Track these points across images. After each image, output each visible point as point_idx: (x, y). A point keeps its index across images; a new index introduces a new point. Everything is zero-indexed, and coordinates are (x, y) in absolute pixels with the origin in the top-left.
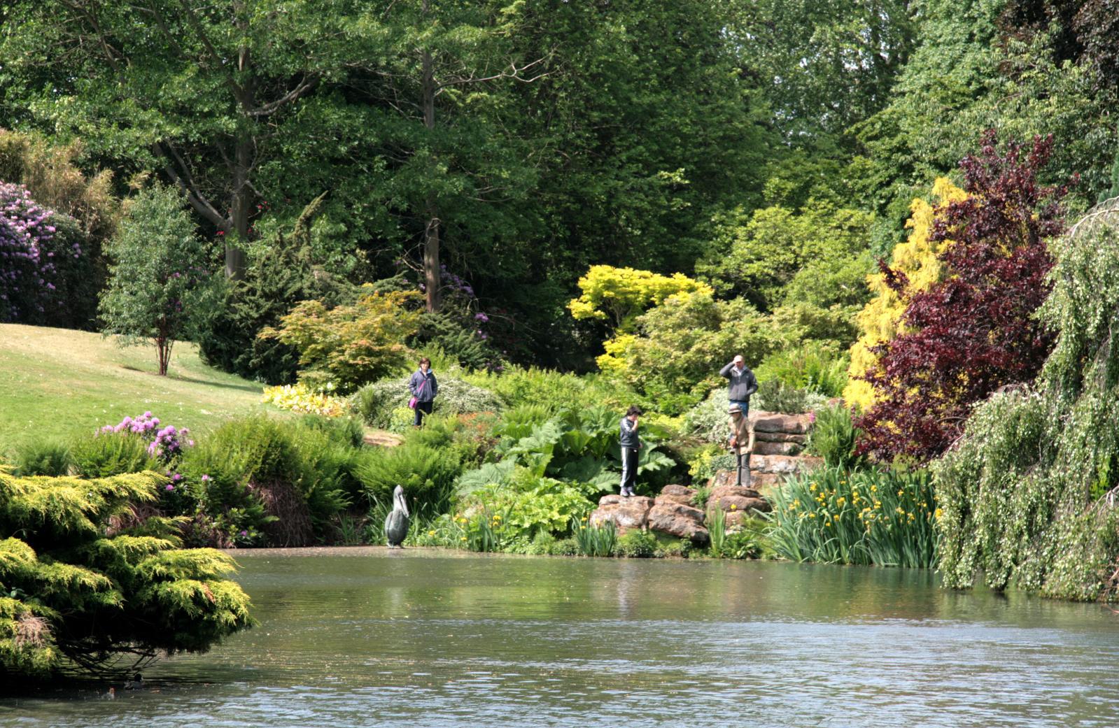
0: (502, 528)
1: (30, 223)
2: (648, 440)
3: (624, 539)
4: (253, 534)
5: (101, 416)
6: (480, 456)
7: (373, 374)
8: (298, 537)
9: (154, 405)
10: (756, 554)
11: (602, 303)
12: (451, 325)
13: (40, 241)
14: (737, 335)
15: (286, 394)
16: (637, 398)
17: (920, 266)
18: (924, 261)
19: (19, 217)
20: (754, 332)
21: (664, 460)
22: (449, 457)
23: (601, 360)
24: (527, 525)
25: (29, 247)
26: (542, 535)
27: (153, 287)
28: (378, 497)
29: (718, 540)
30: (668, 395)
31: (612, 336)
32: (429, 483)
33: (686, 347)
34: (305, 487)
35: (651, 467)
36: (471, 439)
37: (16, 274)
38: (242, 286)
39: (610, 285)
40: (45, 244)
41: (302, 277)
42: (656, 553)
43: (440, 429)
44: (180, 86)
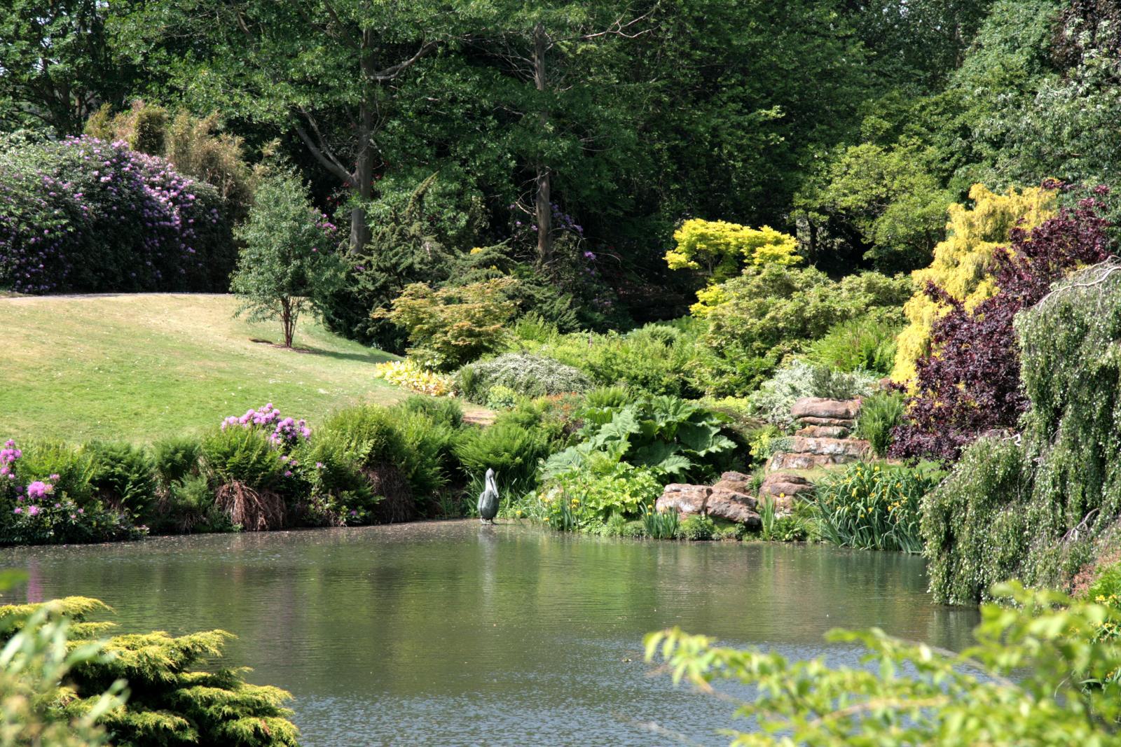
0: (580, 510)
1: (173, 194)
2: (712, 425)
3: (686, 524)
4: (362, 514)
5: (229, 400)
6: (565, 436)
7: (471, 353)
8: (402, 513)
9: (277, 385)
10: (802, 537)
11: (694, 254)
12: (548, 294)
13: (181, 209)
14: (807, 303)
15: (396, 369)
16: (717, 361)
17: (958, 263)
18: (962, 259)
19: (163, 186)
20: (822, 301)
21: (727, 443)
22: (540, 440)
23: (694, 308)
24: (601, 508)
25: (171, 215)
26: (616, 516)
27: (278, 269)
28: (474, 473)
29: (768, 524)
30: (745, 358)
31: (703, 285)
32: (518, 460)
33: (761, 313)
34: (408, 468)
35: (713, 449)
36: (556, 420)
37: (160, 241)
38: (361, 258)
39: (703, 238)
40: (186, 212)
41: (413, 253)
42: (714, 536)
43: (530, 411)
44: (312, 59)
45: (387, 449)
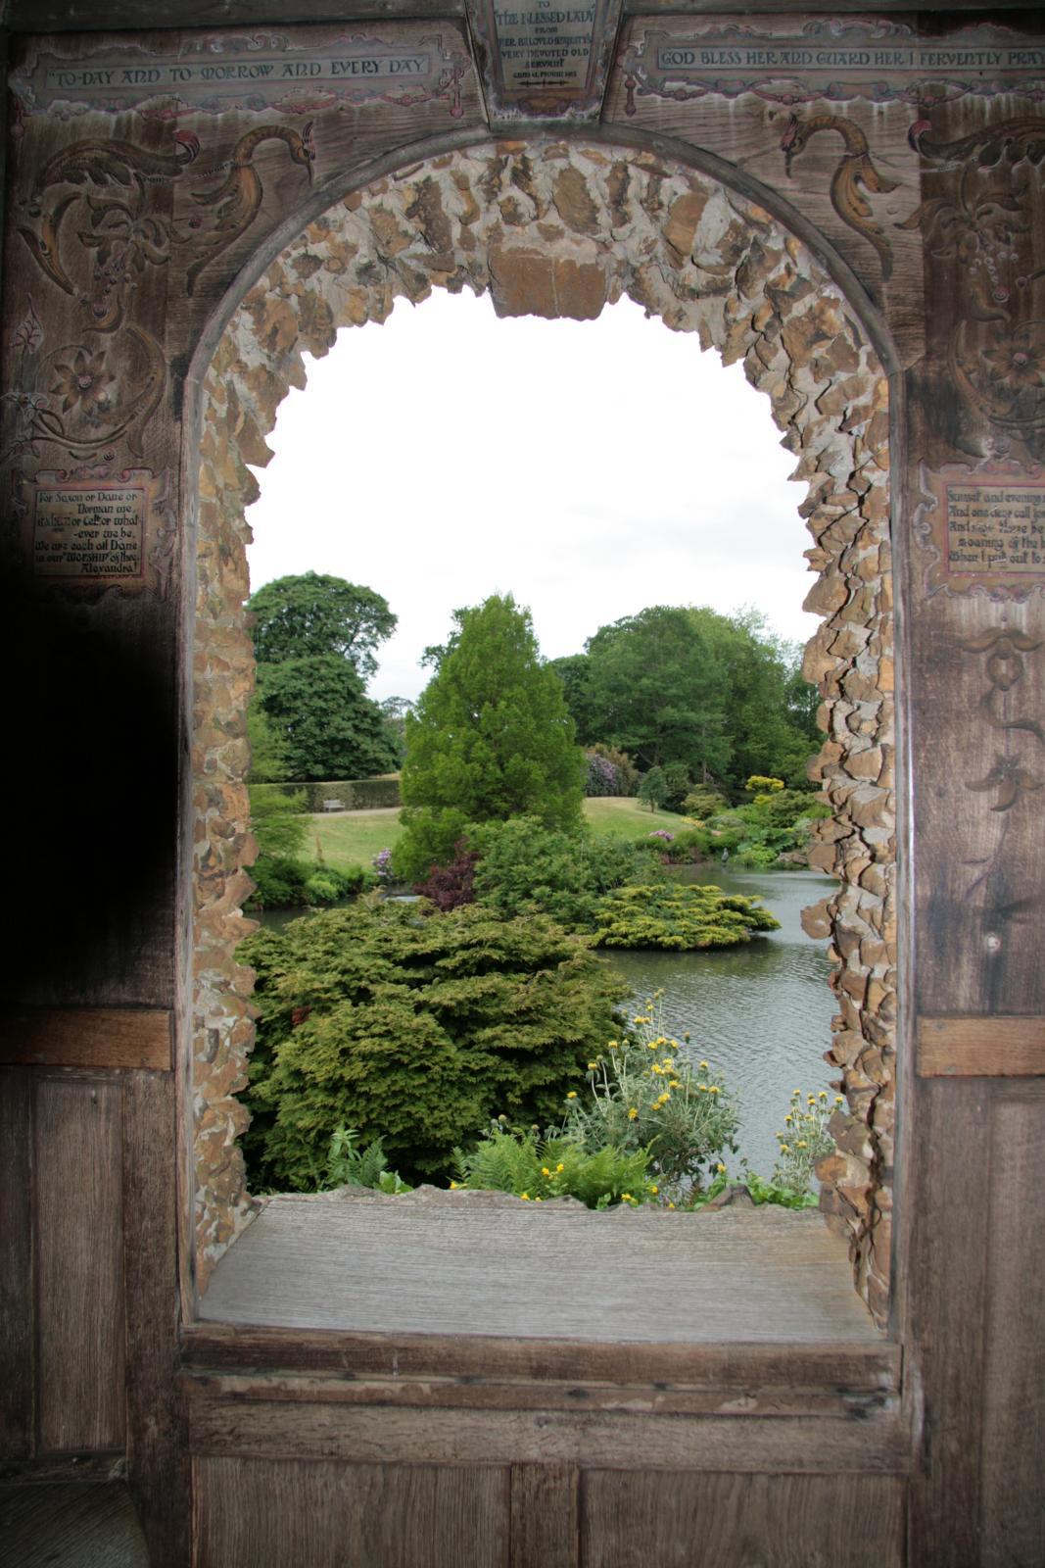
45: (693, 844)
